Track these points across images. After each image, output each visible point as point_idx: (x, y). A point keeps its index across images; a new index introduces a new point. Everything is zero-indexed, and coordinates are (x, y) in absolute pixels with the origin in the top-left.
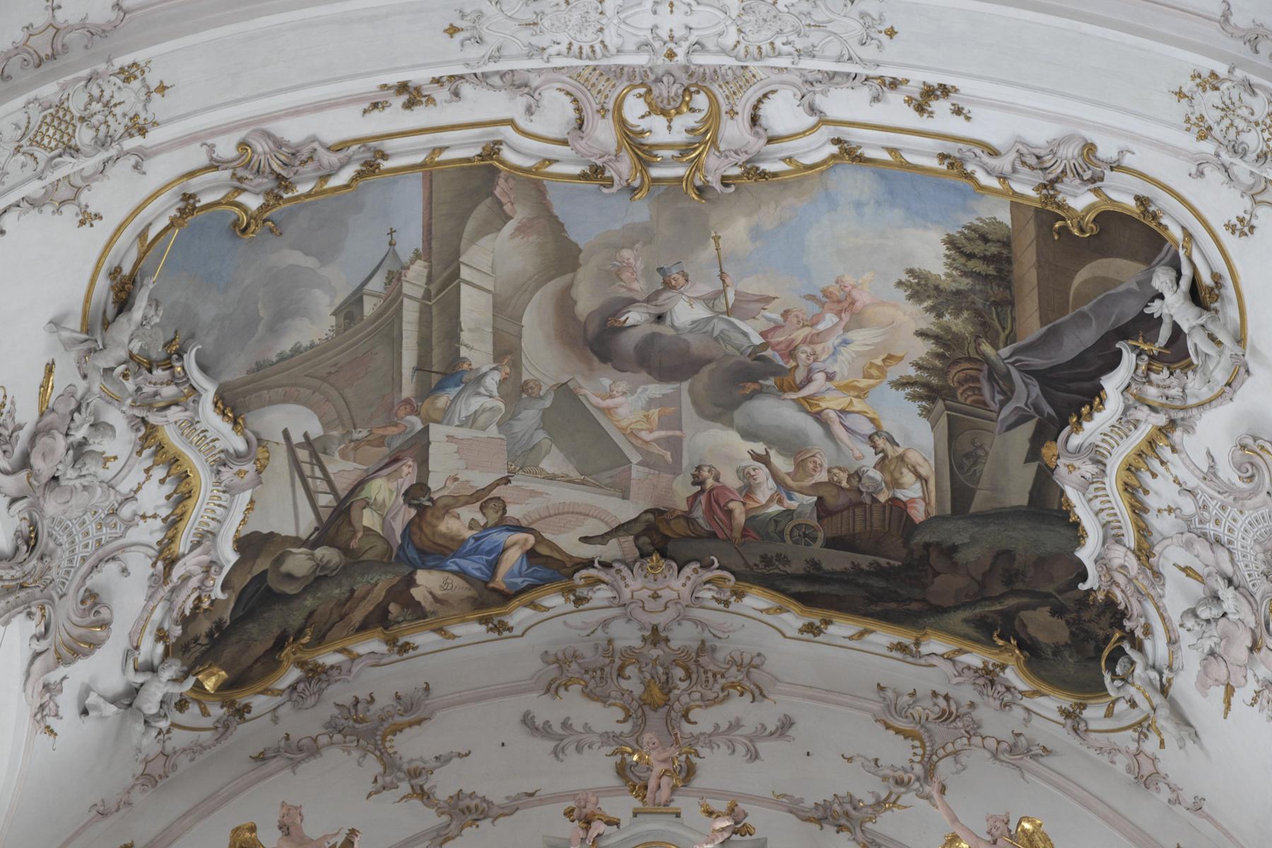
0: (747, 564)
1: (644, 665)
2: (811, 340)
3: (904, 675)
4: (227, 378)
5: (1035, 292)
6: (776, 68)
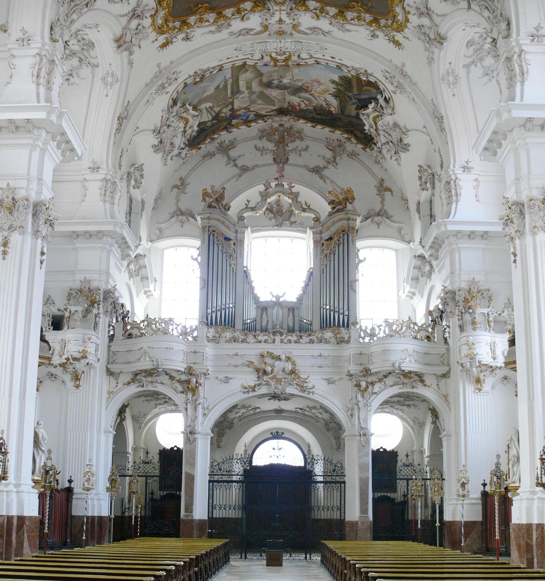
2: (313, 86)
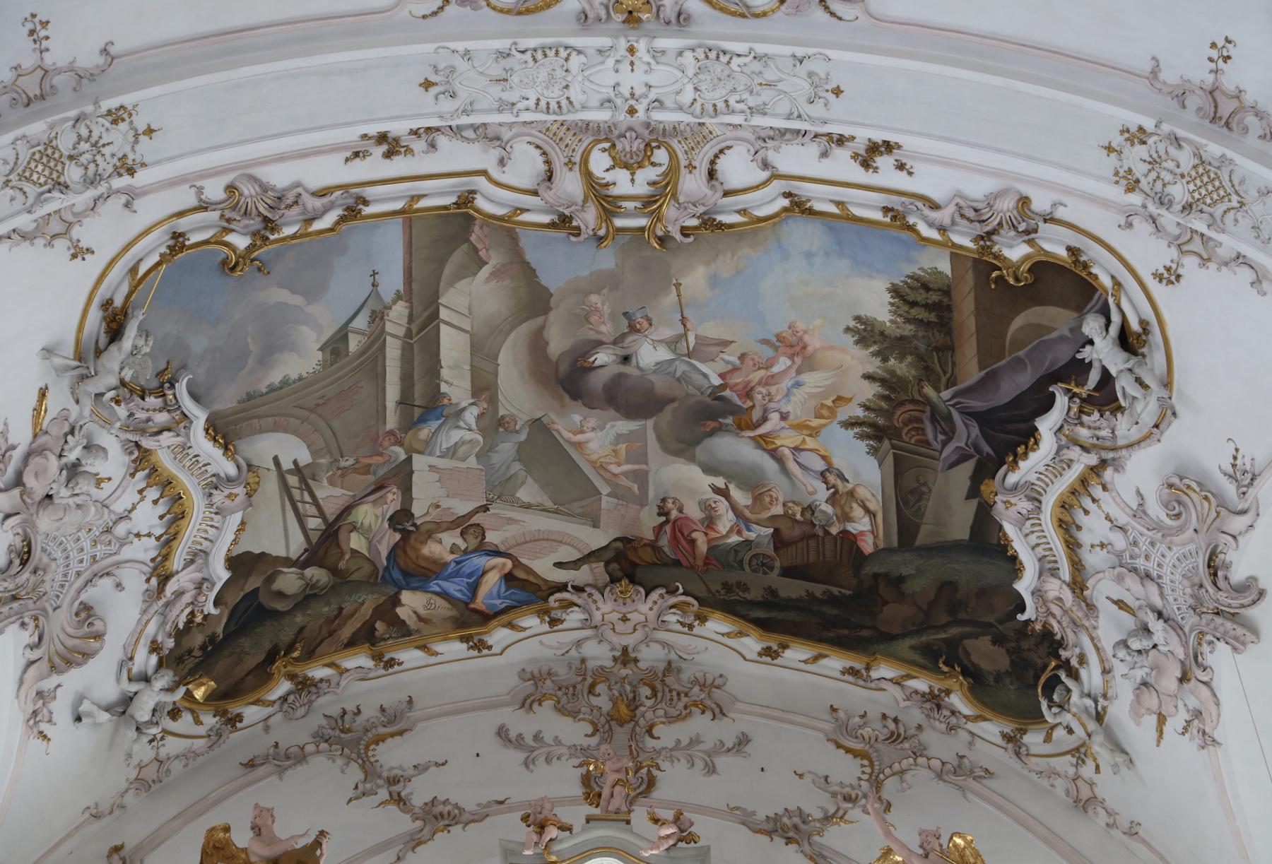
0: (709, 590)
1: (613, 683)
2: (767, 382)
3: (855, 697)
4: (217, 407)
5: (974, 338)
6: (730, 125)
